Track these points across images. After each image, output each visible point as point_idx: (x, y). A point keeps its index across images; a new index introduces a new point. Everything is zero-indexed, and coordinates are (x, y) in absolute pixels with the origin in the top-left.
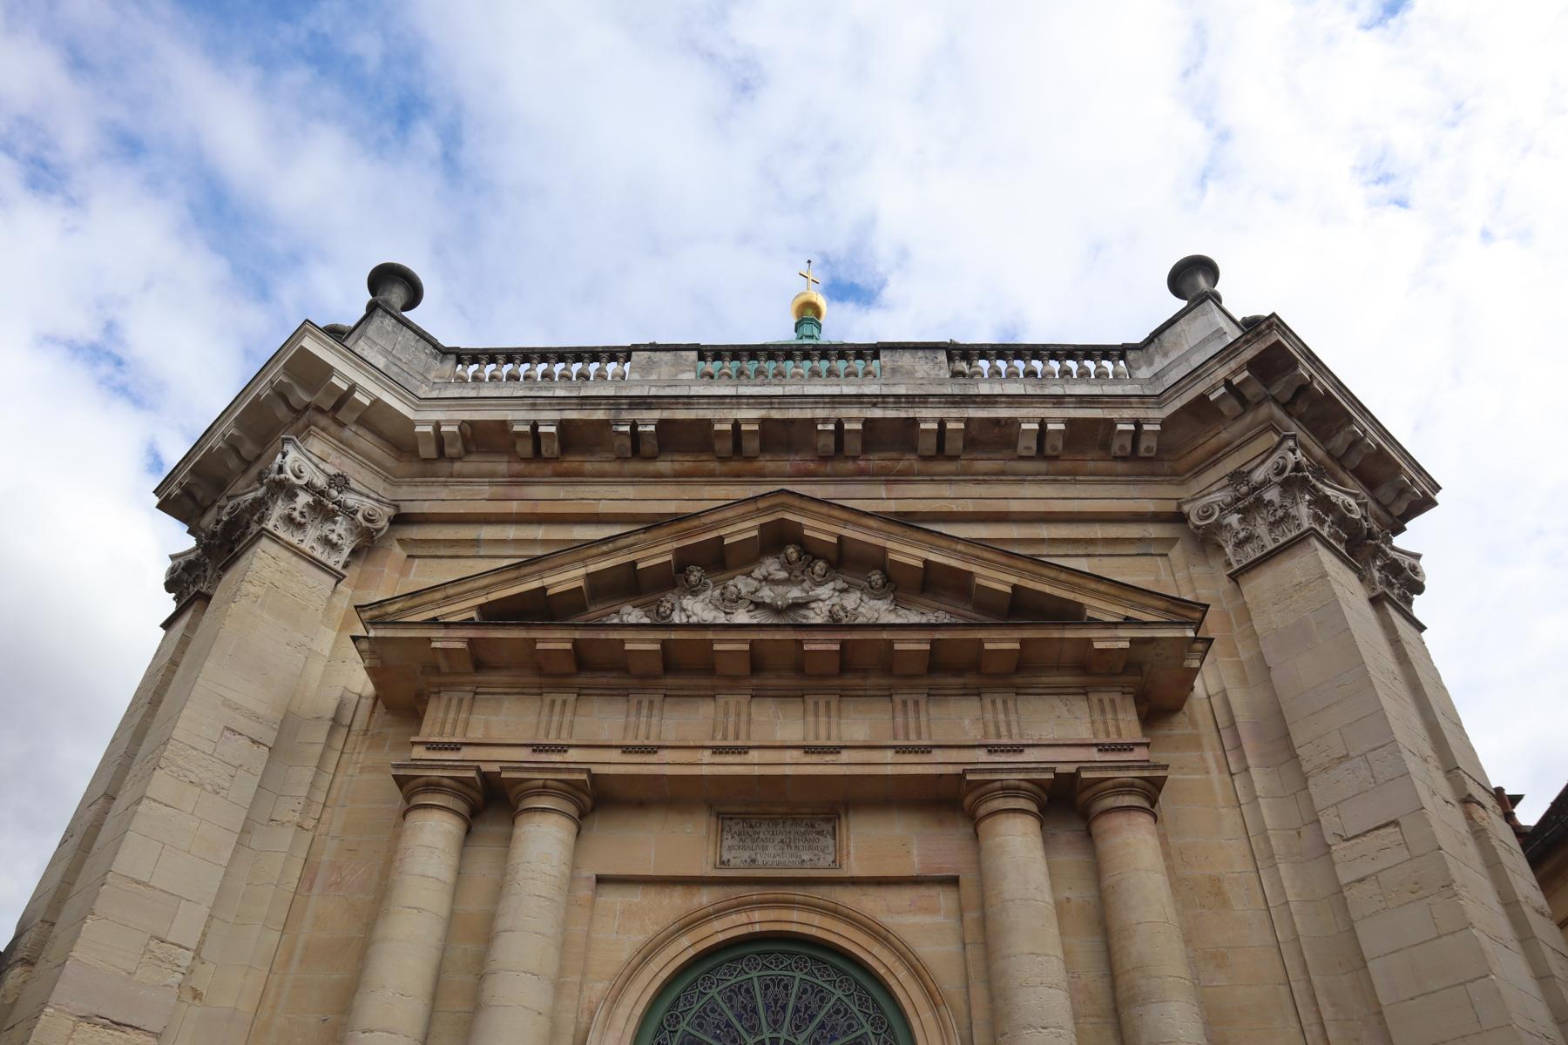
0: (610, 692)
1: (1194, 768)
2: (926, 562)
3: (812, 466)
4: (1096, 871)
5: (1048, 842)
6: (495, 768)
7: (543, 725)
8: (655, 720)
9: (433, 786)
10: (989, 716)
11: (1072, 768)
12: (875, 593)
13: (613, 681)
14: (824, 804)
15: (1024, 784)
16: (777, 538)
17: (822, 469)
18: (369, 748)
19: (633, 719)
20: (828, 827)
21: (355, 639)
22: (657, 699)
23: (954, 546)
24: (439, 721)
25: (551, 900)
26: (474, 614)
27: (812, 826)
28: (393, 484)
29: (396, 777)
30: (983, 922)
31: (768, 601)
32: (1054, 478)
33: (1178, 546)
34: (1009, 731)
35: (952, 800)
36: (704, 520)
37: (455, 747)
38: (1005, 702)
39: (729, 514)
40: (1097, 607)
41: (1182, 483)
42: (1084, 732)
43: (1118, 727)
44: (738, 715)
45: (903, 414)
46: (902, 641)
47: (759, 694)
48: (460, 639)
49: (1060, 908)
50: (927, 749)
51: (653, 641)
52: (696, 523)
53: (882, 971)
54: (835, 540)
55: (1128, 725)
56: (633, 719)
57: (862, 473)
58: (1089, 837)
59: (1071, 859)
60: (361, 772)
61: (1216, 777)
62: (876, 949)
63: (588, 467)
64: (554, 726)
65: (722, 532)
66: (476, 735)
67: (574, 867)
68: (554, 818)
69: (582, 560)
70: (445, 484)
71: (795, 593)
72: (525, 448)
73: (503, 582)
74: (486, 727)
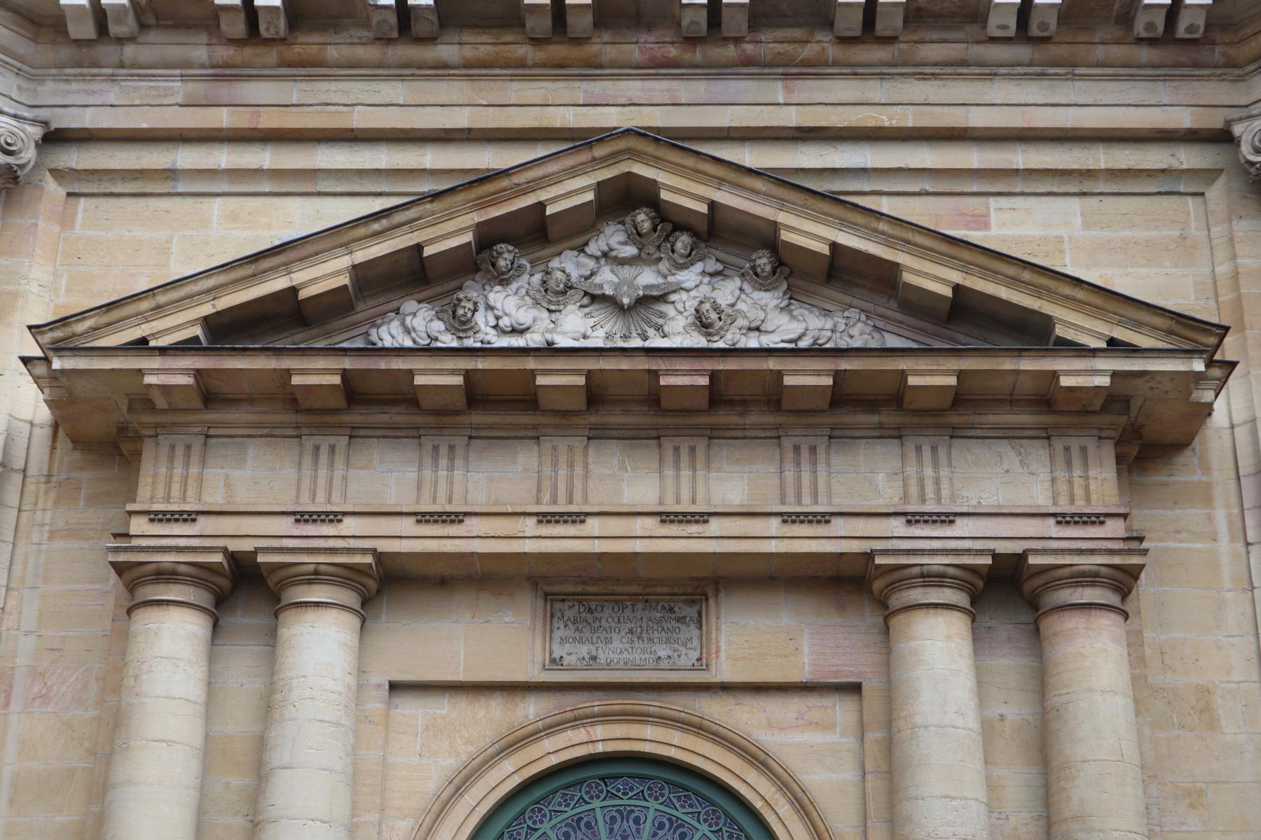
0: (392, 433)
1: (1194, 534)
2: (834, 246)
3: (673, 52)
4: (1041, 682)
5: (978, 638)
6: (247, 546)
7: (306, 483)
8: (458, 474)
9: (166, 575)
10: (911, 470)
11: (1017, 547)
12: (761, 281)
13: (398, 419)
14: (686, 589)
15: (951, 571)
16: (622, 199)
17: (687, 56)
18: (57, 502)
19: (428, 473)
20: (691, 612)
21: (26, 361)
22: (460, 442)
23: (874, 224)
24: (162, 480)
25: (338, 724)
26: (197, 331)
27: (671, 610)
28: (31, 78)
29: (114, 565)
30: (890, 745)
31: (609, 291)
32: (1038, 72)
33: (1220, 183)
34: (938, 492)
35: (857, 585)
36: (517, 179)
37: (189, 517)
38: (934, 449)
39: (552, 168)
41: (1240, 79)
42: (1038, 494)
43: (1087, 489)
44: (571, 466)
46: (795, 372)
47: (598, 434)
48: (185, 371)
49: (988, 729)
50: (824, 518)
51: (453, 372)
52: (505, 183)
53: (758, 804)
54: (703, 208)
55: (1100, 483)
56: (428, 473)
57: (749, 62)
58: (1036, 636)
59: (1009, 664)
60: (50, 538)
61: (1226, 546)
62: (752, 776)
63: (332, 53)
64: (322, 482)
65: (543, 196)
66: (215, 498)
67: (361, 671)
68: (333, 614)
69: (345, 245)
70: (112, 78)
71: (647, 278)
72: (237, 27)
73: (236, 282)
74: (228, 486)
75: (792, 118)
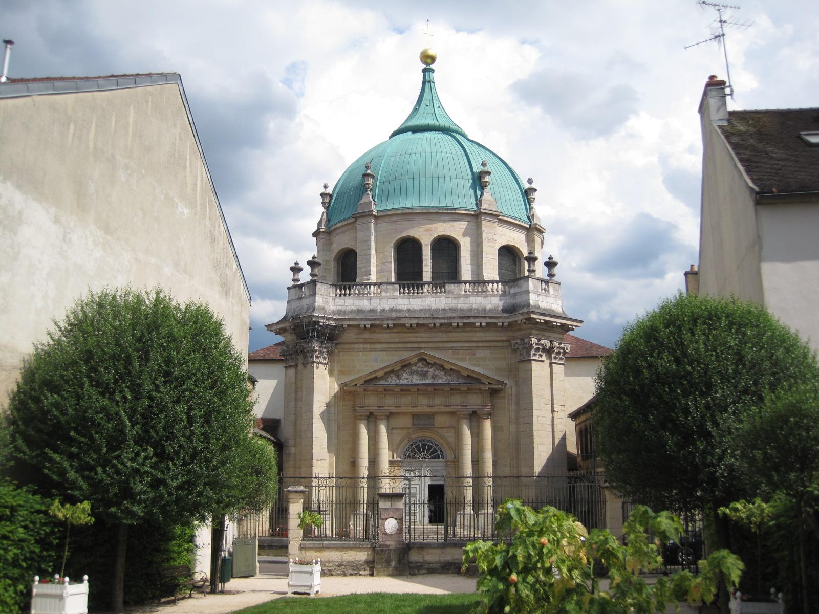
37: (364, 407)
40: (484, 380)
45: (449, 322)
71: (425, 369)
75: (446, 339)
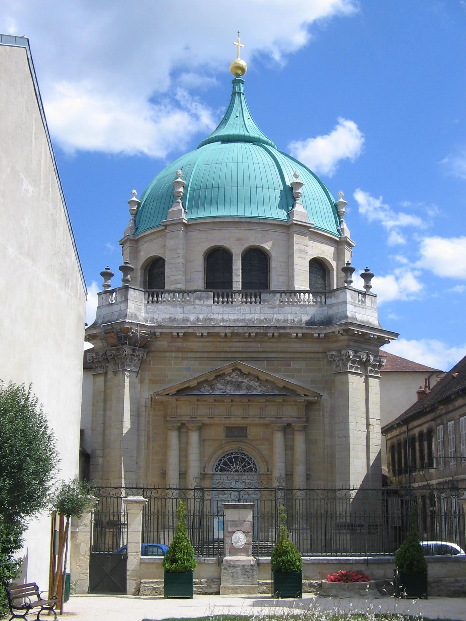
37: (175, 417)
40: (300, 391)
45: (264, 332)
71: (240, 380)
75: (261, 350)
